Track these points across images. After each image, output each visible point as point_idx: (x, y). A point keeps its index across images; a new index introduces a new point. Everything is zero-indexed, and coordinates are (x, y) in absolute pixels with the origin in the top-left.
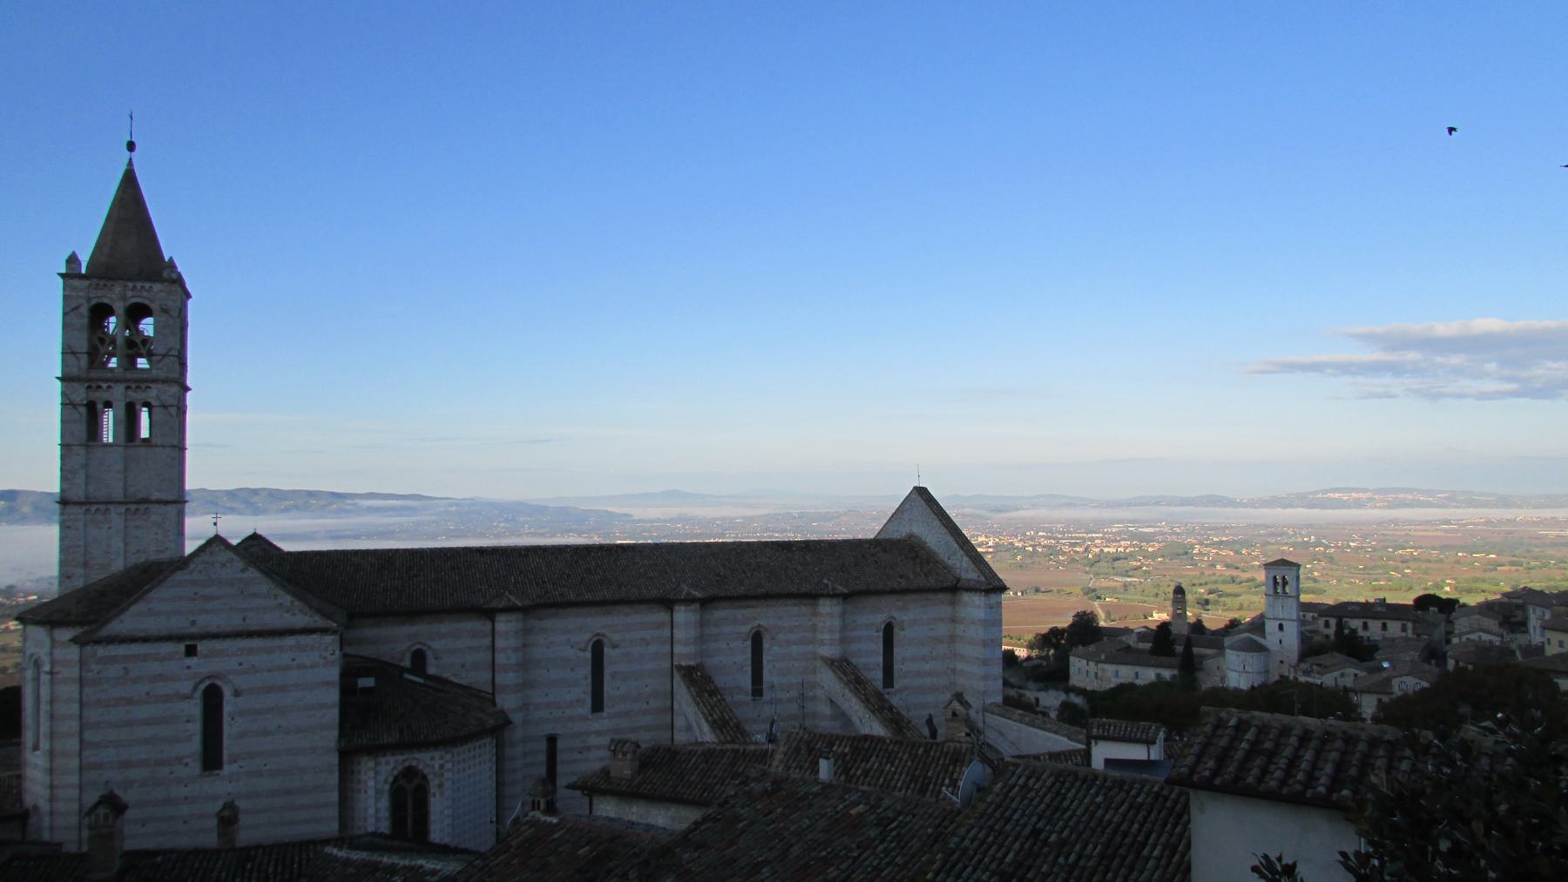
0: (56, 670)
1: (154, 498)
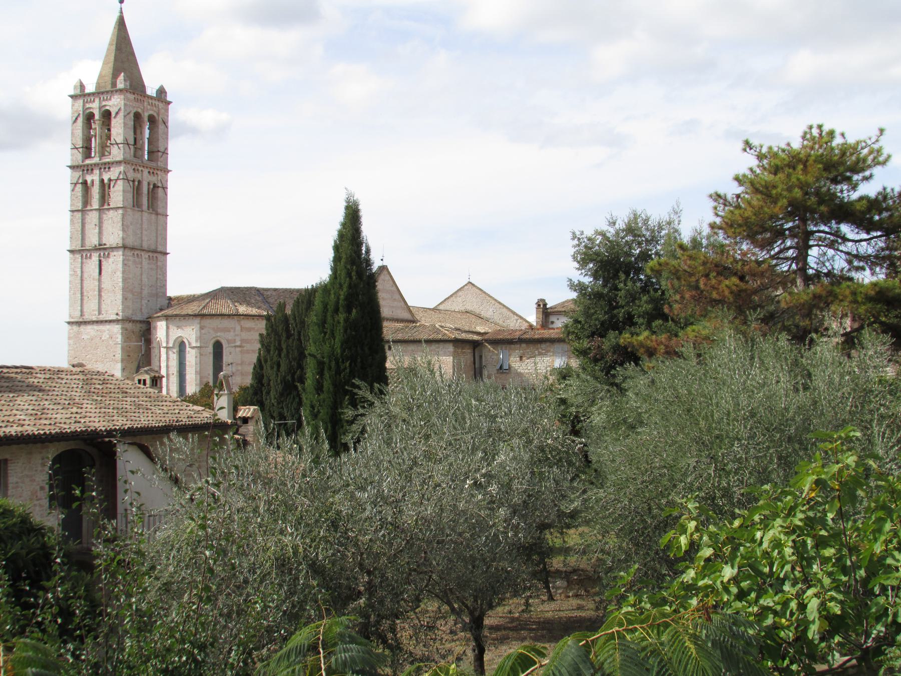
0: (243, 344)
1: (159, 250)
